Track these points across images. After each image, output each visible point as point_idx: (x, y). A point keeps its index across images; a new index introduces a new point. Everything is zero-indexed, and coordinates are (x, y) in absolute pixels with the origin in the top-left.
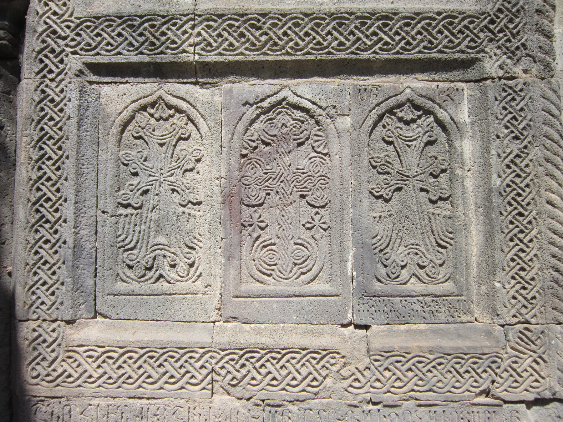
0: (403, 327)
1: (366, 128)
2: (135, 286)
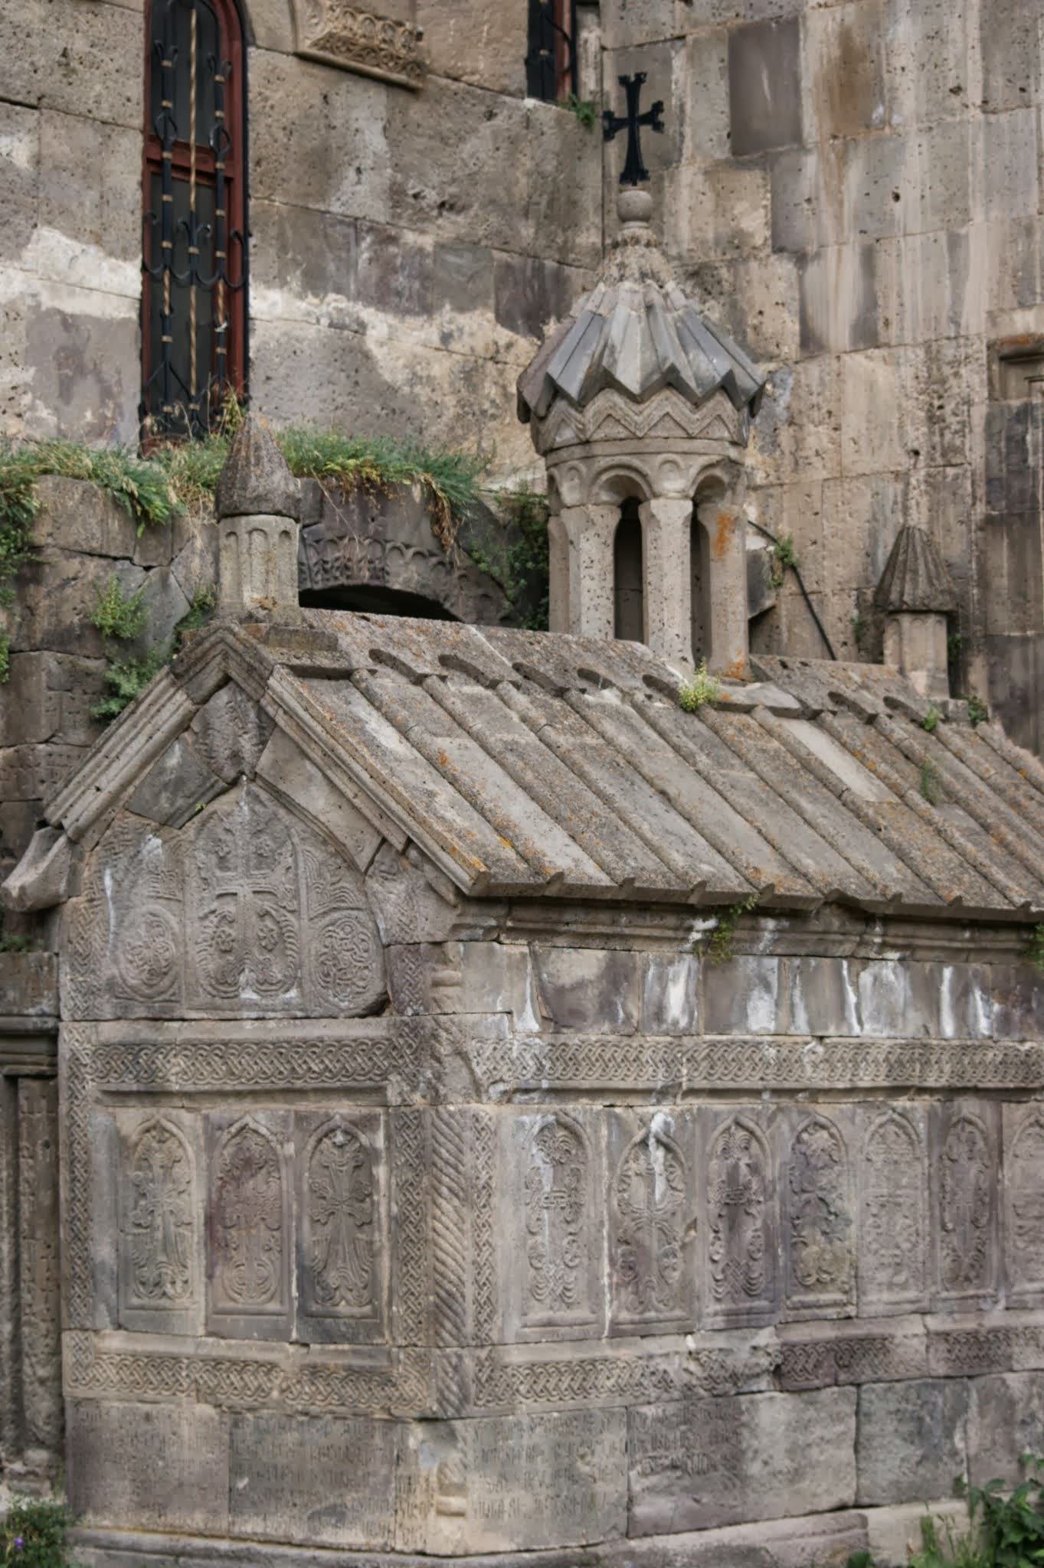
0: (332, 1347)
1: (307, 1154)
2: (145, 1301)
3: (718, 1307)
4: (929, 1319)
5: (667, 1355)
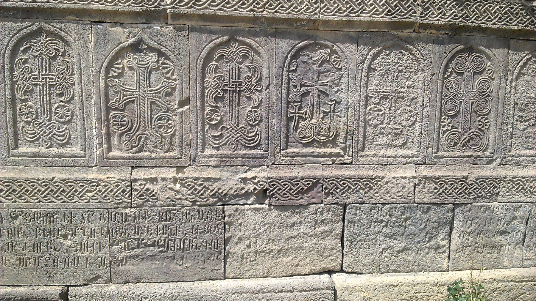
3: (214, 152)
4: (422, 167)
5: (155, 179)
